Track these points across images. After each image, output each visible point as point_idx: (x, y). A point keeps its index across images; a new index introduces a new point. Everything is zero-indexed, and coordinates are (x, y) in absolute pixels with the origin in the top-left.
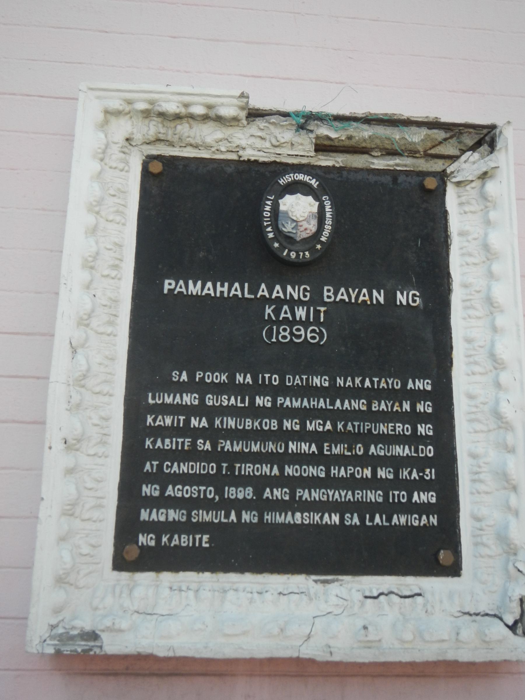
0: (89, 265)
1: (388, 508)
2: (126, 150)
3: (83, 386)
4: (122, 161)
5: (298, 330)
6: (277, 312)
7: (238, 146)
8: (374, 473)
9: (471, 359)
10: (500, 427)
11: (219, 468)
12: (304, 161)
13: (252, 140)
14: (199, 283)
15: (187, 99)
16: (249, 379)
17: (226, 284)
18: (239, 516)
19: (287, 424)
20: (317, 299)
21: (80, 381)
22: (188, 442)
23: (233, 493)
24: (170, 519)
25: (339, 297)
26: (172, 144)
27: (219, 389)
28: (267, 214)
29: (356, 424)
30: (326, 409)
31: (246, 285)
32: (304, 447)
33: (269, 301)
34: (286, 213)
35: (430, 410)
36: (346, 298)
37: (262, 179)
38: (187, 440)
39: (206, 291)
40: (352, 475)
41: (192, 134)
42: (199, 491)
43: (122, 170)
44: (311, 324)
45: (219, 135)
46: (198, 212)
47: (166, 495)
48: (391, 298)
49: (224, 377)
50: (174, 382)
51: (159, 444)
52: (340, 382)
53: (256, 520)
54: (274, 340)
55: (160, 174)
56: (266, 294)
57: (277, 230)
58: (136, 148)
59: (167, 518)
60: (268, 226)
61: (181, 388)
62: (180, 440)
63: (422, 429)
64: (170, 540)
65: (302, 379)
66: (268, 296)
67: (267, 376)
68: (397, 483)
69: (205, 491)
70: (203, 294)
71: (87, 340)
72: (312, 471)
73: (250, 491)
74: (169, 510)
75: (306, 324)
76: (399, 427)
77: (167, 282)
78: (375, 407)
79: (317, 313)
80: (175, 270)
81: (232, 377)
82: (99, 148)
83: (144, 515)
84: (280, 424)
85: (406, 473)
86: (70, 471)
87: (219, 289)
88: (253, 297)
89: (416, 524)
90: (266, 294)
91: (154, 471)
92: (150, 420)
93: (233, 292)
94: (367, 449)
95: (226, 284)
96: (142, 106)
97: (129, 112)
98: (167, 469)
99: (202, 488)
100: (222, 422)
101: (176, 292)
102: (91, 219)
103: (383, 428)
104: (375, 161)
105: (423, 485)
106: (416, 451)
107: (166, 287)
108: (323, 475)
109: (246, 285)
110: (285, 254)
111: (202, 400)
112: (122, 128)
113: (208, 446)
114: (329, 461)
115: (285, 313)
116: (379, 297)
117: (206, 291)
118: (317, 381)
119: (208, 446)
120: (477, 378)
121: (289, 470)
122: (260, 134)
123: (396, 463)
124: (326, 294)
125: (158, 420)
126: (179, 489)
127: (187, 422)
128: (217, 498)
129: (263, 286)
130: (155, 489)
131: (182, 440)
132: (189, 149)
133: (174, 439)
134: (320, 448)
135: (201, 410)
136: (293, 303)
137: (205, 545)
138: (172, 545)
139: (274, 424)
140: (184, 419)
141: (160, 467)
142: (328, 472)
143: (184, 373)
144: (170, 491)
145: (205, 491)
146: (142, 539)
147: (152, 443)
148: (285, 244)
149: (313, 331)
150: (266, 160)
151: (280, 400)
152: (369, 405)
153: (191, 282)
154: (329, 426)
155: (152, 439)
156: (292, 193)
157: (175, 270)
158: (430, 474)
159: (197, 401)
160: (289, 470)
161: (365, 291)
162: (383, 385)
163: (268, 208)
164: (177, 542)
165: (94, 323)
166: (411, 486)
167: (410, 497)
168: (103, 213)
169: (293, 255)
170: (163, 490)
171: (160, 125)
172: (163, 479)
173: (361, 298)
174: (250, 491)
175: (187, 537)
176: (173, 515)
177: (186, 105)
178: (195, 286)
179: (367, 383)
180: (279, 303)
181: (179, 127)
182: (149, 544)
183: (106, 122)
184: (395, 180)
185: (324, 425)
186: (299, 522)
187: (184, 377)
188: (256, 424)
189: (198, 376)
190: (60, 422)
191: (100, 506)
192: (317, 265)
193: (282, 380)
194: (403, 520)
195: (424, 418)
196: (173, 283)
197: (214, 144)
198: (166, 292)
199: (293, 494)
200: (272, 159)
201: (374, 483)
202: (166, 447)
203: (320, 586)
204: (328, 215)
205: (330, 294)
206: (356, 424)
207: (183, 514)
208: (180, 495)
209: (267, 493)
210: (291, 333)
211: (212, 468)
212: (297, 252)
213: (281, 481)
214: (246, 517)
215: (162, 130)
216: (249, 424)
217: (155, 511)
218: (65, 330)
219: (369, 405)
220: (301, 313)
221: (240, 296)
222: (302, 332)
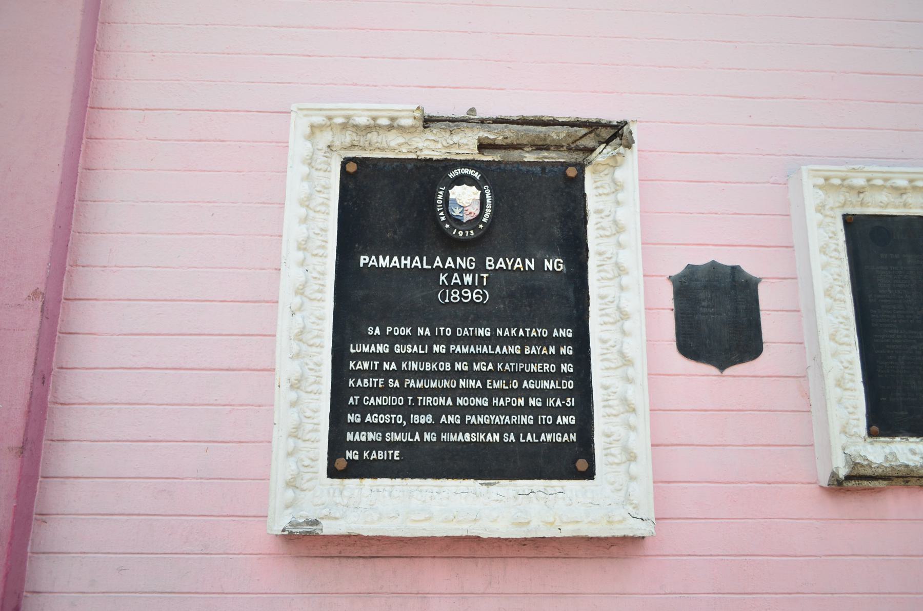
0: (302, 246)
1: (538, 429)
2: (328, 154)
3: (301, 340)
4: (325, 163)
5: (466, 292)
6: (449, 279)
8: (527, 402)
9: (603, 312)
10: (625, 365)
11: (406, 401)
12: (470, 157)
13: (427, 143)
14: (388, 258)
15: (375, 114)
16: (428, 332)
17: (409, 258)
18: (422, 437)
19: (458, 366)
20: (480, 267)
21: (300, 336)
23: (416, 419)
24: (370, 439)
25: (498, 266)
26: (364, 149)
27: (404, 340)
28: (439, 202)
29: (512, 364)
30: (489, 354)
32: (472, 383)
33: (443, 270)
34: (455, 200)
35: (571, 353)
36: (503, 266)
40: (509, 404)
41: (380, 140)
42: (391, 418)
43: (325, 171)
44: (476, 287)
45: (401, 140)
48: (540, 264)
49: (408, 331)
51: (359, 383)
52: (499, 332)
53: (435, 439)
54: (447, 301)
55: (356, 172)
56: (440, 264)
61: (375, 340)
62: (375, 380)
63: (564, 368)
64: (370, 455)
65: (469, 331)
67: (442, 329)
68: (544, 409)
71: (302, 305)
72: (478, 401)
73: (430, 417)
75: (472, 288)
76: (546, 367)
77: (362, 257)
78: (527, 351)
79: (481, 278)
81: (414, 331)
83: (349, 437)
84: (453, 366)
85: (551, 402)
86: (293, 404)
87: (403, 262)
89: (559, 440)
90: (440, 264)
92: (352, 365)
93: (414, 264)
94: (521, 384)
95: (409, 258)
96: (340, 120)
99: (393, 416)
102: (303, 211)
103: (533, 368)
104: (527, 155)
105: (565, 411)
106: (560, 385)
108: (486, 404)
112: (325, 138)
113: (397, 384)
114: (491, 394)
115: (456, 279)
117: (393, 264)
118: (481, 332)
119: (397, 384)
120: (609, 327)
121: (460, 401)
123: (543, 394)
124: (488, 263)
127: (380, 366)
128: (405, 423)
129: (438, 258)
132: (377, 151)
134: (484, 384)
136: (462, 271)
139: (448, 366)
141: (360, 400)
142: (490, 402)
143: (377, 328)
144: (368, 419)
146: (349, 454)
148: (454, 225)
149: (478, 293)
150: (439, 158)
151: (452, 347)
152: (523, 350)
153: (381, 257)
154: (490, 367)
158: (570, 402)
160: (460, 401)
161: (519, 260)
162: (534, 333)
163: (440, 197)
165: (308, 292)
166: (556, 412)
167: (555, 420)
168: (311, 206)
169: (461, 233)
170: (363, 418)
171: (354, 134)
172: (363, 410)
173: (516, 266)
174: (430, 417)
176: (371, 436)
178: (384, 259)
179: (521, 333)
180: (451, 271)
181: (369, 135)
183: (313, 133)
184: (543, 169)
185: (487, 366)
186: (468, 440)
187: (377, 331)
188: (434, 366)
190: (287, 369)
191: (316, 431)
192: (480, 241)
193: (454, 332)
194: (549, 437)
195: (566, 359)
196: (367, 258)
197: (397, 147)
198: (361, 265)
199: (463, 419)
200: (444, 157)
203: (485, 487)
204: (488, 201)
205: (492, 263)
206: (512, 364)
210: (461, 295)
211: (400, 401)
212: (464, 232)
214: (427, 437)
216: (428, 366)
218: (287, 297)
219: (523, 350)
220: (468, 279)
222: (469, 294)
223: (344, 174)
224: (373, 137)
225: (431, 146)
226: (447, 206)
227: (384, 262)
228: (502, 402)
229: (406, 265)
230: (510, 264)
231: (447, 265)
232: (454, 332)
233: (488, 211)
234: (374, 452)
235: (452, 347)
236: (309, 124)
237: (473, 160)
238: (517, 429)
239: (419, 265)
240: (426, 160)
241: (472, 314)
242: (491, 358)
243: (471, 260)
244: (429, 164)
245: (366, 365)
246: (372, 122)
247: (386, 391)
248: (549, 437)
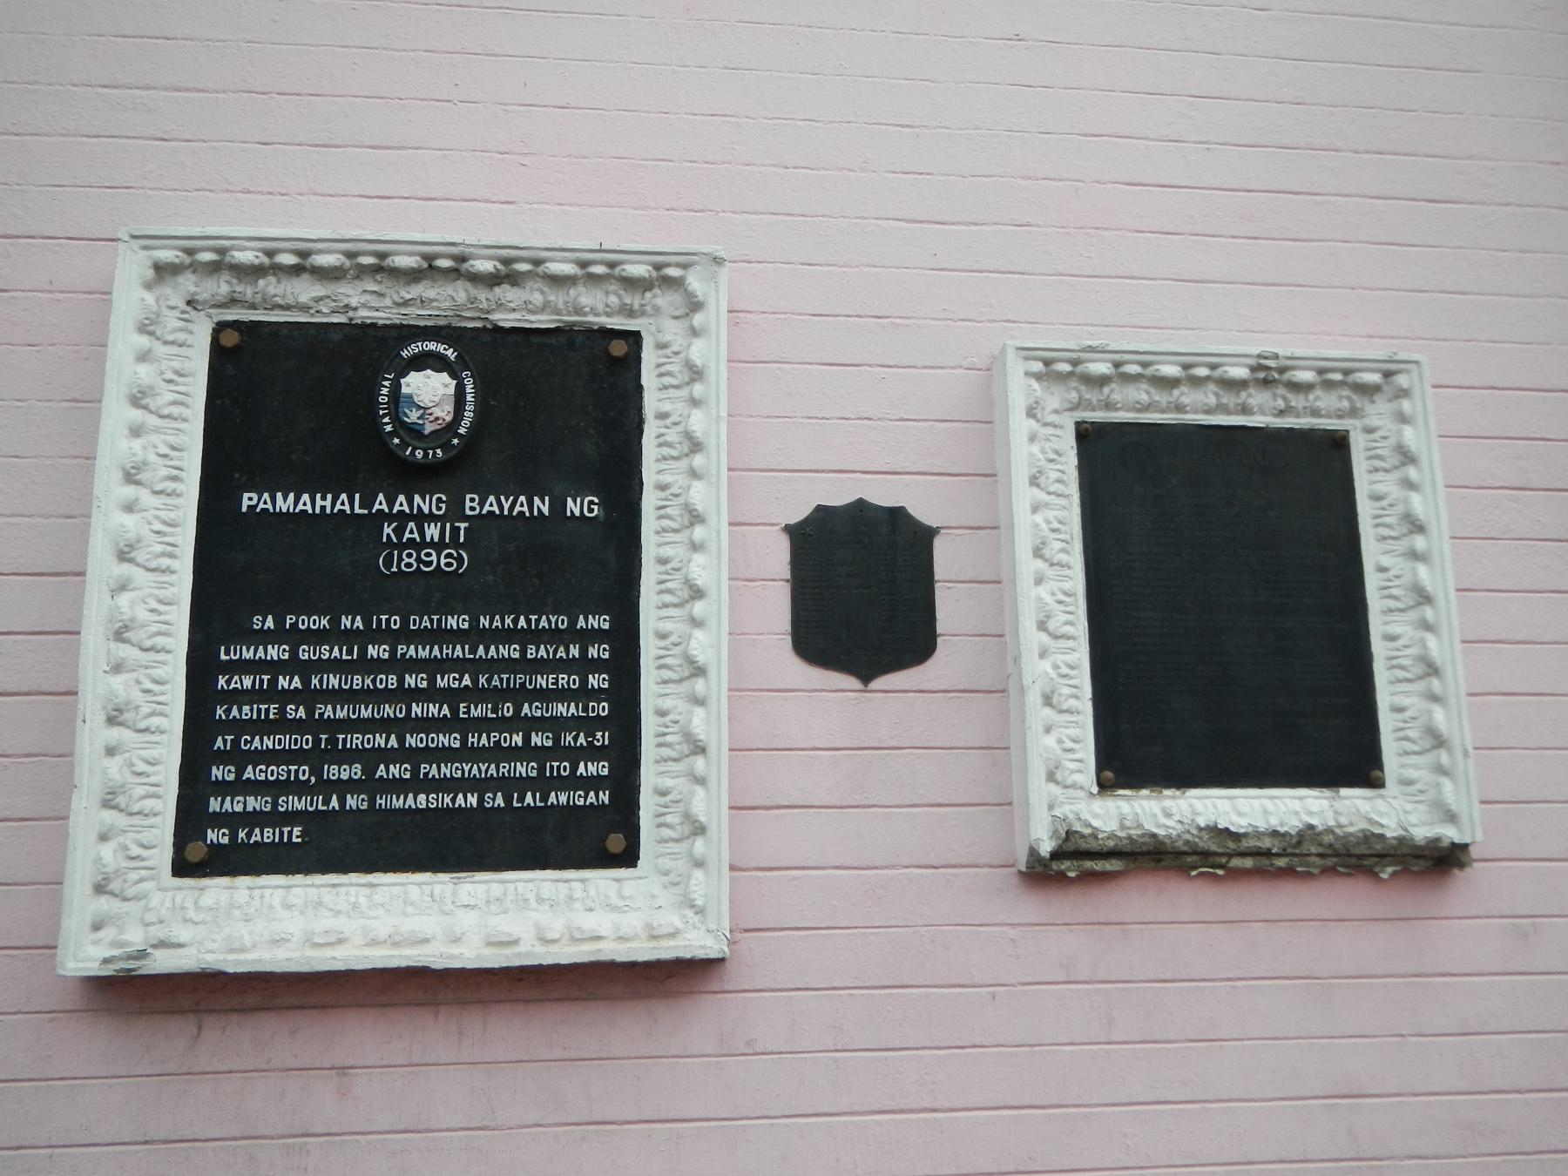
1: (543, 784)
5: (428, 555)
6: (399, 531)
7: (346, 306)
8: (527, 739)
11: (317, 741)
14: (292, 495)
16: (359, 623)
17: (329, 496)
18: (342, 802)
19: (410, 681)
23: (333, 772)
24: (250, 809)
25: (487, 508)
26: (253, 306)
27: (317, 637)
28: (383, 399)
29: (505, 676)
30: (465, 659)
32: (433, 710)
33: (390, 517)
34: (410, 397)
37: (379, 350)
39: (300, 507)
42: (289, 772)
46: (289, 397)
48: (558, 506)
49: (324, 622)
51: (235, 712)
53: (365, 806)
54: (394, 569)
56: (385, 507)
60: (385, 415)
61: (265, 638)
62: (263, 707)
64: (249, 835)
65: (431, 621)
67: (384, 617)
68: (558, 751)
69: (297, 771)
72: (443, 740)
75: (439, 546)
76: (563, 679)
77: (246, 495)
81: (335, 621)
83: (214, 805)
84: (401, 681)
85: (569, 738)
87: (319, 502)
90: (385, 507)
92: (222, 681)
93: (338, 507)
94: (518, 709)
95: (329, 496)
97: (191, 265)
99: (293, 768)
100: (321, 681)
103: (541, 681)
105: (592, 753)
113: (302, 713)
116: (543, 506)
117: (300, 507)
118: (452, 622)
119: (302, 713)
121: (411, 741)
122: (375, 288)
123: (556, 725)
124: (468, 504)
128: (313, 779)
129: (381, 497)
135: (292, 666)
136: (422, 519)
137: (295, 840)
141: (236, 743)
143: (270, 618)
144: (249, 773)
145: (297, 771)
146: (211, 836)
149: (449, 556)
151: (401, 649)
152: (523, 652)
153: (279, 495)
154: (467, 681)
156: (419, 370)
160: (411, 741)
161: (522, 498)
163: (385, 391)
167: (574, 768)
169: (419, 454)
170: (240, 772)
173: (518, 508)
176: (253, 803)
178: (285, 499)
179: (522, 623)
180: (402, 518)
185: (460, 680)
187: (270, 623)
188: (368, 681)
192: (453, 465)
193: (405, 622)
196: (255, 496)
197: (311, 304)
198: (244, 509)
199: (415, 771)
201: (526, 752)
204: (469, 398)
208: (263, 777)
209: (381, 771)
210: (419, 560)
212: (425, 450)
213: (404, 754)
214: (351, 802)
215: (239, 289)
216: (357, 681)
219: (523, 652)
220: (432, 532)
222: (434, 558)
223: (220, 355)
225: (369, 304)
226: (397, 407)
227: (284, 504)
228: (484, 740)
229: (323, 508)
230: (506, 506)
231: (396, 508)
232: (405, 622)
233: (469, 415)
234: (257, 831)
235: (401, 649)
236: (149, 263)
237: (448, 327)
238: (507, 785)
239: (347, 508)
240: (364, 326)
241: (438, 591)
242: (469, 666)
243: (439, 500)
244: (372, 332)
245: (247, 682)
246: (265, 260)
247: (282, 725)
248: (563, 799)
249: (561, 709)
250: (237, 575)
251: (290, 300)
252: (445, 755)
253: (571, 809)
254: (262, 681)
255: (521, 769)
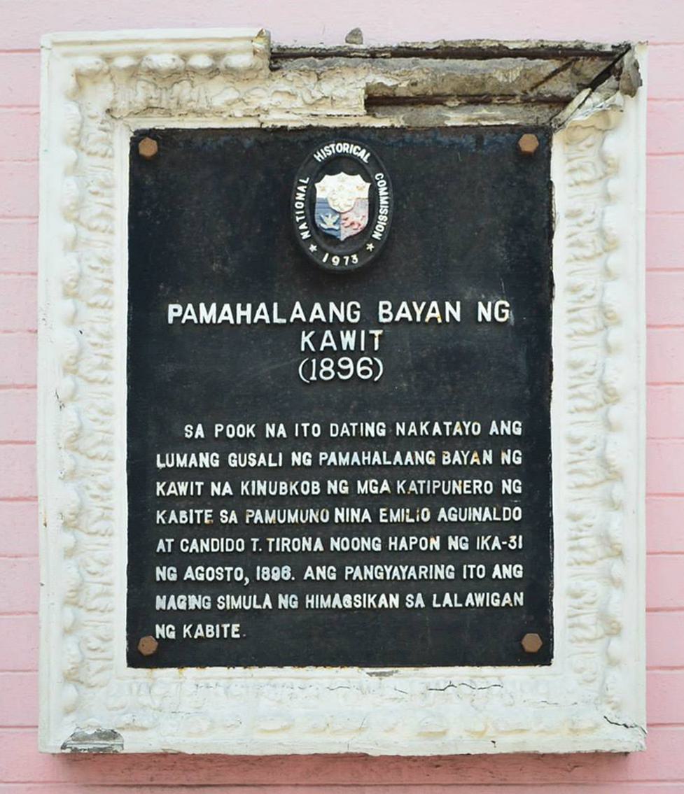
1: (461, 586)
2: (107, 126)
3: (76, 450)
4: (103, 140)
5: (345, 363)
6: (317, 340)
8: (444, 543)
11: (249, 545)
14: (214, 307)
16: (282, 431)
17: (249, 306)
18: (275, 601)
19: (332, 487)
21: (74, 442)
22: (209, 513)
23: (265, 573)
24: (192, 607)
25: (399, 315)
27: (244, 445)
28: (299, 205)
29: (421, 482)
30: (383, 466)
31: (275, 305)
32: (355, 515)
33: (307, 326)
34: (325, 202)
38: (207, 511)
39: (222, 317)
41: (195, 97)
42: (225, 573)
43: (104, 156)
46: (205, 206)
47: (185, 579)
48: (470, 311)
49: (250, 430)
50: (187, 438)
51: (173, 517)
53: (295, 605)
54: (313, 378)
56: (302, 316)
57: (313, 226)
58: (120, 122)
59: (188, 606)
60: (301, 222)
61: (196, 446)
62: (199, 512)
64: (193, 631)
65: (350, 428)
66: (304, 319)
68: (473, 554)
69: (232, 572)
70: (220, 321)
71: (75, 390)
72: (365, 543)
74: (189, 596)
75: (355, 354)
76: (478, 485)
77: (171, 307)
80: (181, 290)
81: (260, 430)
82: (73, 129)
83: (160, 603)
84: (324, 487)
85: (484, 542)
86: (69, 553)
87: (240, 313)
88: (284, 321)
90: (302, 316)
91: (169, 550)
92: (160, 488)
93: (258, 316)
94: (435, 514)
95: (249, 306)
96: (124, 62)
98: (184, 548)
99: (229, 569)
100: (249, 487)
101: (183, 321)
102: (70, 229)
103: (456, 487)
105: (507, 556)
107: (171, 316)
109: (275, 305)
110: (325, 260)
111: (224, 461)
112: (100, 97)
113: (233, 518)
116: (454, 311)
117: (222, 317)
118: (370, 429)
119: (233, 518)
121: (335, 544)
122: (287, 89)
123: (471, 530)
124: (381, 311)
125: (170, 488)
126: (200, 571)
127: (206, 488)
128: (247, 580)
129: (298, 306)
130: (172, 572)
131: (202, 511)
132: (191, 117)
133: (191, 511)
135: (223, 473)
136: (337, 327)
137: (234, 636)
138: (196, 637)
140: (202, 486)
141: (175, 545)
143: (200, 427)
144: (189, 574)
145: (232, 572)
146: (160, 631)
147: (164, 516)
148: (324, 246)
151: (323, 456)
152: (439, 458)
153: (202, 306)
154: (385, 487)
155: (164, 512)
156: (332, 173)
157: (181, 290)
159: (217, 462)
160: (335, 544)
161: (434, 304)
163: (300, 197)
164: (202, 634)
165: (84, 368)
167: (490, 571)
169: (336, 261)
170: (181, 573)
171: (151, 87)
172: (180, 560)
173: (430, 315)
175: (212, 627)
176: (195, 602)
177: (185, 57)
178: (208, 310)
179: (437, 429)
180: (319, 326)
182: (169, 636)
183: (80, 87)
185: (379, 486)
187: (200, 432)
188: (293, 487)
189: (217, 430)
191: (108, 594)
192: (368, 272)
193: (325, 430)
196: (180, 308)
197: (225, 107)
198: (170, 321)
199: (340, 573)
201: (443, 556)
202: (181, 522)
204: (383, 201)
207: (206, 600)
208: (202, 578)
209: (309, 573)
210: (336, 368)
212: (341, 257)
213: (327, 557)
214: (283, 601)
217: (172, 597)
219: (439, 458)
220: (348, 339)
221: (268, 321)
222: (351, 366)
224: (183, 90)
227: (208, 315)
228: (403, 544)
229: (244, 318)
230: (419, 313)
231: (313, 317)
232: (325, 430)
233: (383, 219)
234: (200, 627)
235: (323, 456)
238: (429, 587)
239: (266, 317)
241: (355, 399)
242: (387, 472)
243: (354, 307)
244: (281, 136)
245: (183, 488)
247: (216, 529)
248: (480, 600)
249: (476, 514)
250: (167, 385)
251: (203, 105)
252: (366, 558)
253: (488, 610)
254: (195, 487)
255: (439, 572)
